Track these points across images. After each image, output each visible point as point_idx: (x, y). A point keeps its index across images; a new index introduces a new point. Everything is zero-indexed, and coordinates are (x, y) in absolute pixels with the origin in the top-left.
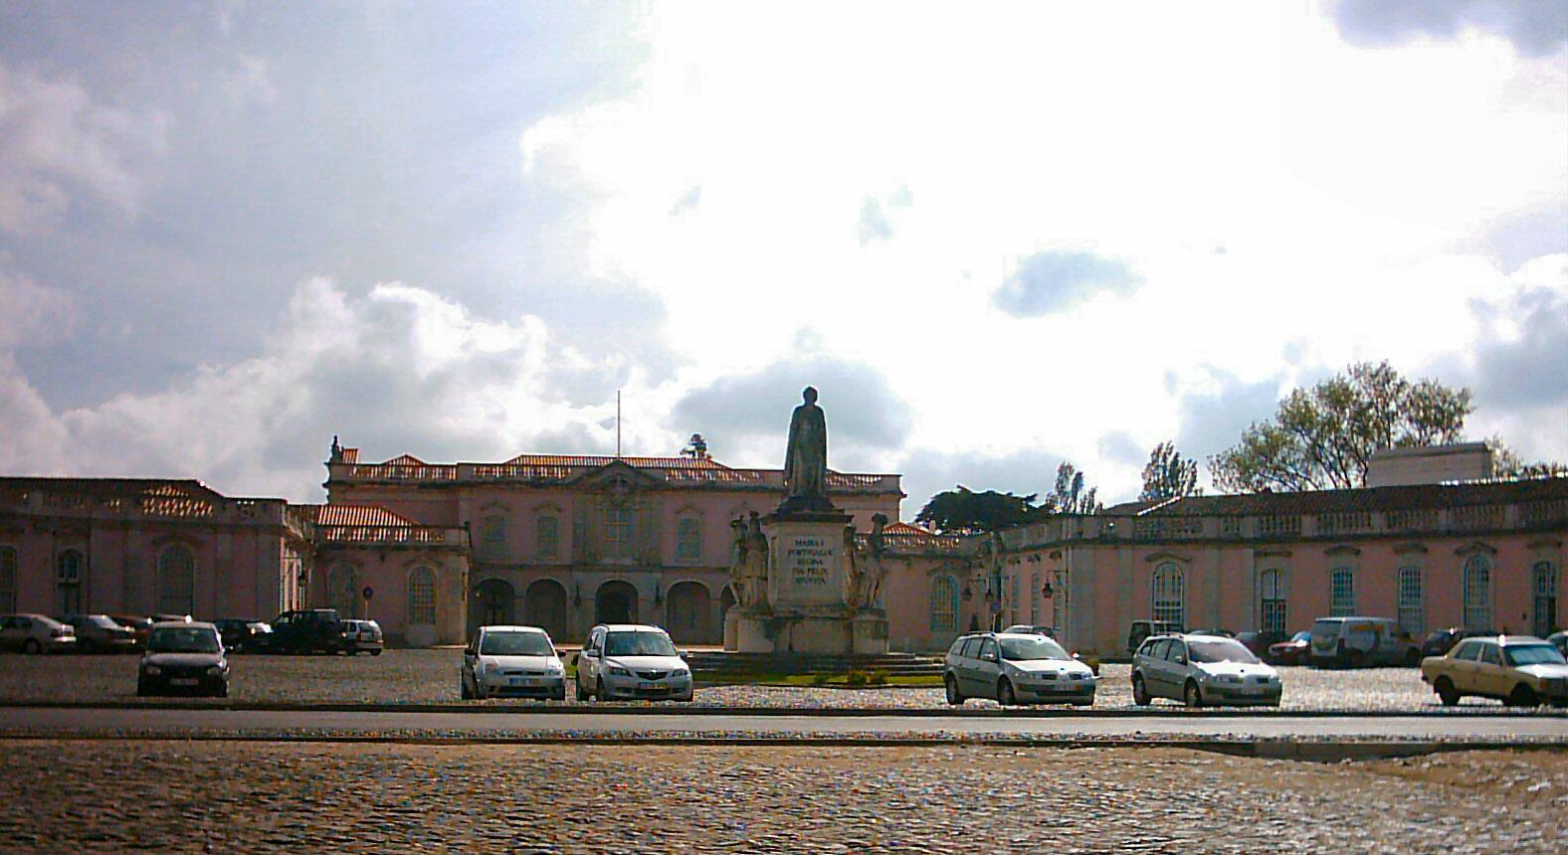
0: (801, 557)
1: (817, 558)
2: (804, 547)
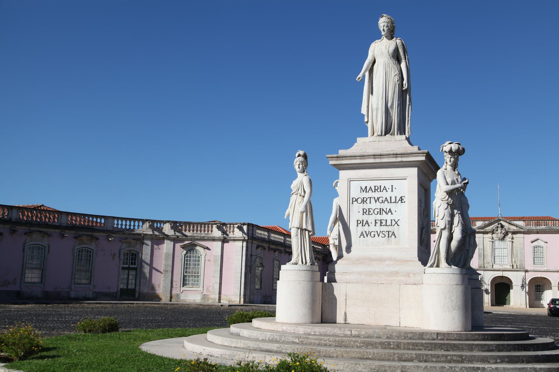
0: (367, 206)
1: (386, 206)
2: (370, 194)
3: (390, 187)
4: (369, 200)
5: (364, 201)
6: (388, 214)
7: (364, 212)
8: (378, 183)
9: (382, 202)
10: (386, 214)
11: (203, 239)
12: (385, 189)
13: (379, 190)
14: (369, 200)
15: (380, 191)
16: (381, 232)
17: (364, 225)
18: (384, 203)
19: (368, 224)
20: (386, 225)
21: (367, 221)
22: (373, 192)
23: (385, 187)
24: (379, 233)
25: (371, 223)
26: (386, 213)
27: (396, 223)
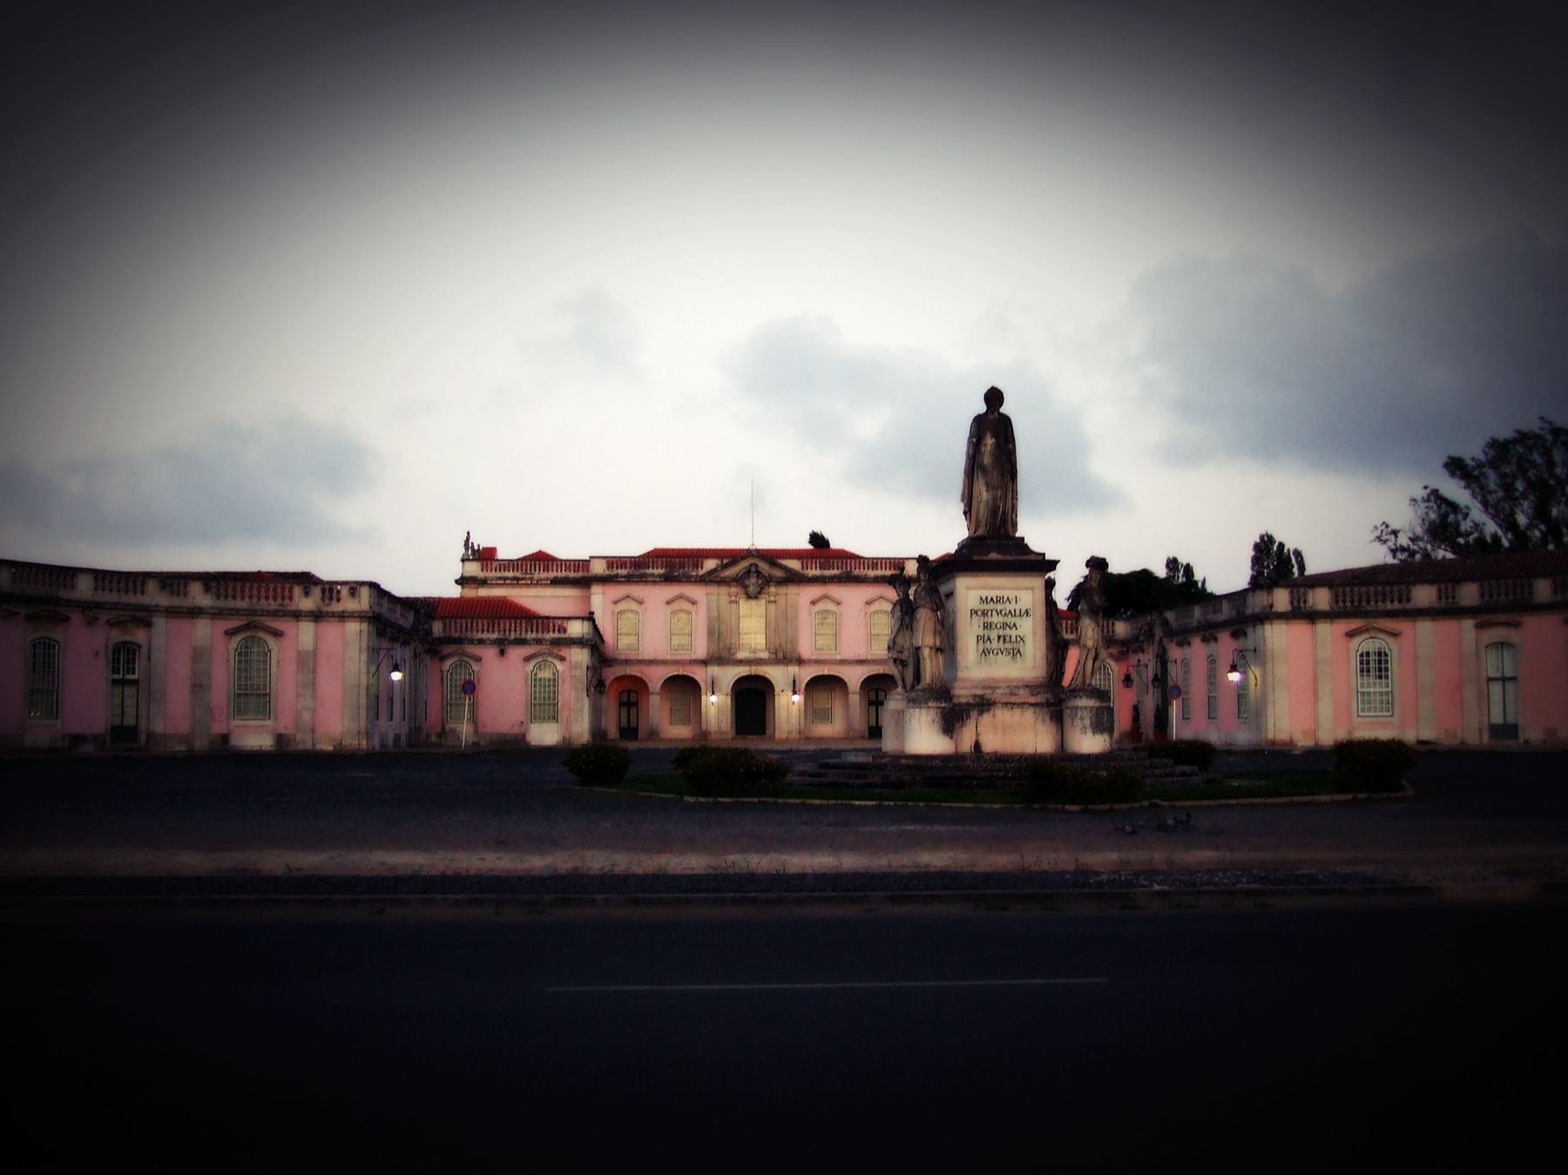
1: (1009, 620)
2: (991, 606)
8: (1000, 593)
11: (274, 614)
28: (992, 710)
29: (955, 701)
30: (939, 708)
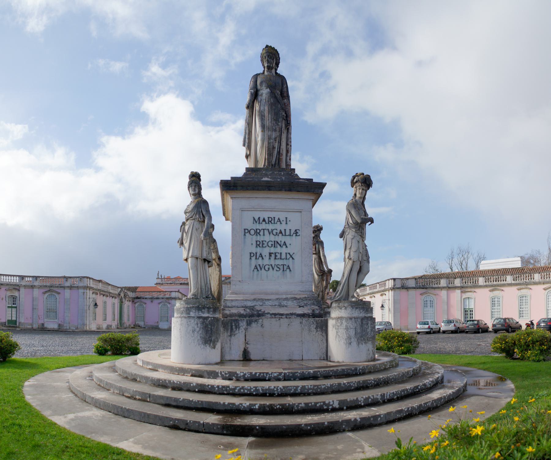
1: (280, 239)
2: (264, 226)
3: (285, 219)
4: (262, 231)
5: (257, 232)
6: (282, 247)
7: (257, 245)
8: (272, 215)
9: (277, 234)
10: (280, 247)
12: (278, 221)
13: (273, 222)
14: (262, 231)
15: (274, 223)
16: (276, 266)
17: (257, 258)
18: (278, 235)
19: (262, 256)
20: (281, 259)
21: (261, 254)
22: (266, 223)
23: (279, 219)
24: (273, 266)
25: (265, 256)
26: (280, 245)
27: (291, 256)
28: (260, 321)
29: (227, 312)
30: (199, 318)
